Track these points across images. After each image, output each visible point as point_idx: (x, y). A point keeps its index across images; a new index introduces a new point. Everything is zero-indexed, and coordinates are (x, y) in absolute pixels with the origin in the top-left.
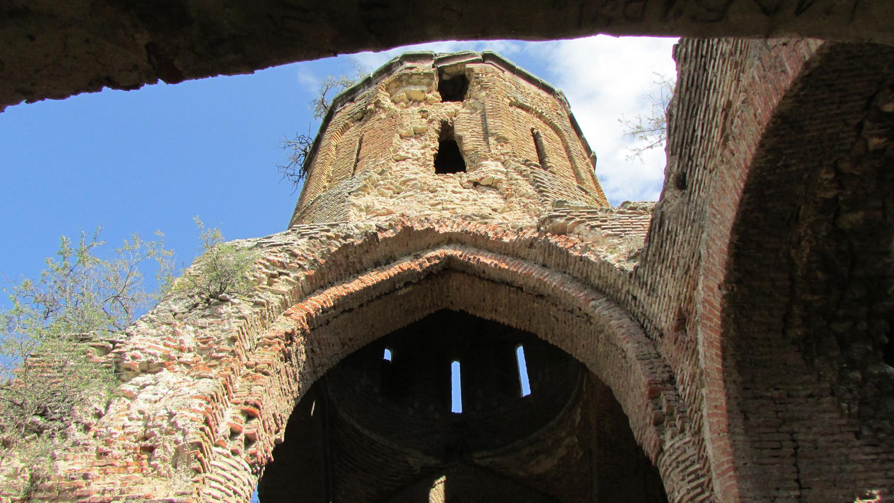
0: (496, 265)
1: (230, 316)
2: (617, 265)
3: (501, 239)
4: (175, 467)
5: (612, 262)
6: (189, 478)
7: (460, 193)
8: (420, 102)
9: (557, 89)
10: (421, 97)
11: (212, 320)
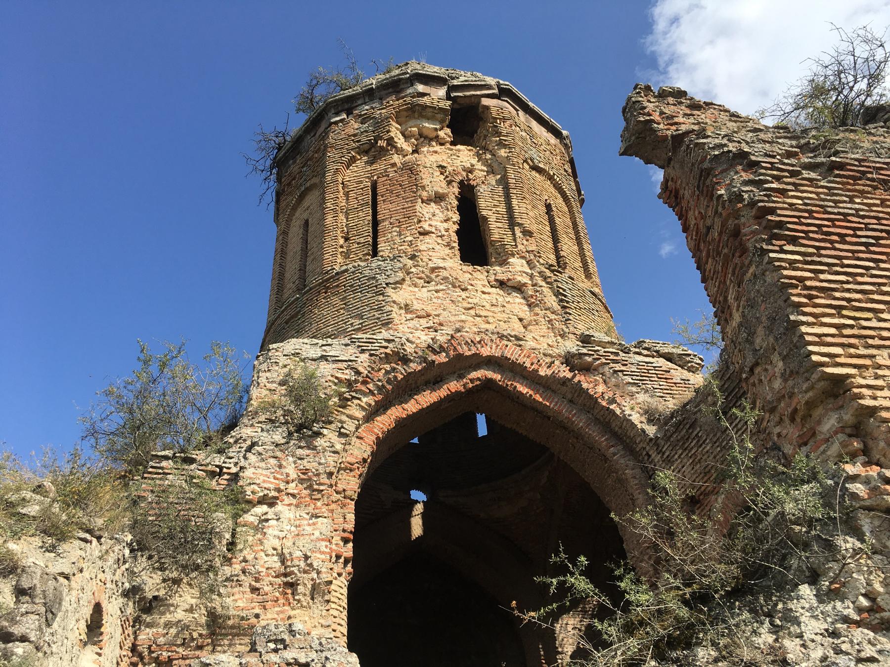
0: (531, 395)
1: (325, 450)
2: (639, 426)
3: (537, 371)
4: (312, 599)
5: (636, 422)
6: (323, 608)
7: (489, 293)
8: (431, 140)
9: (565, 133)
10: (433, 134)
11: (308, 452)
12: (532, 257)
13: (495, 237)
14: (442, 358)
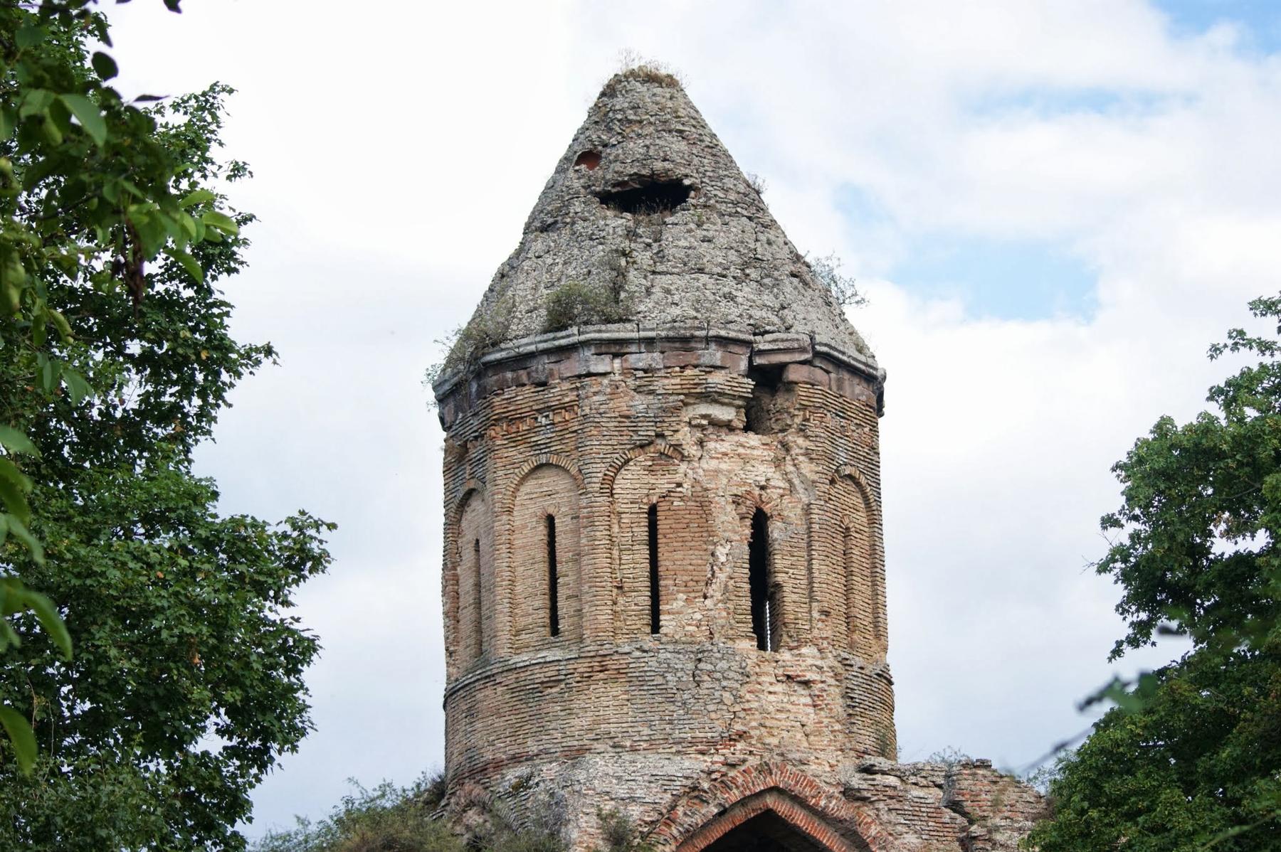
12: (825, 644)
13: (789, 617)
14: (735, 795)
